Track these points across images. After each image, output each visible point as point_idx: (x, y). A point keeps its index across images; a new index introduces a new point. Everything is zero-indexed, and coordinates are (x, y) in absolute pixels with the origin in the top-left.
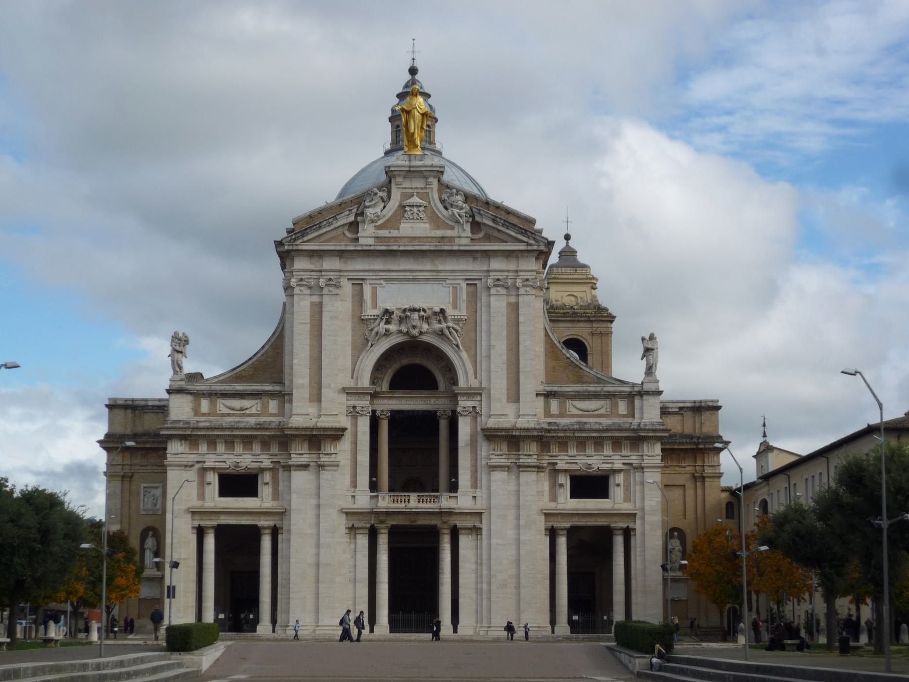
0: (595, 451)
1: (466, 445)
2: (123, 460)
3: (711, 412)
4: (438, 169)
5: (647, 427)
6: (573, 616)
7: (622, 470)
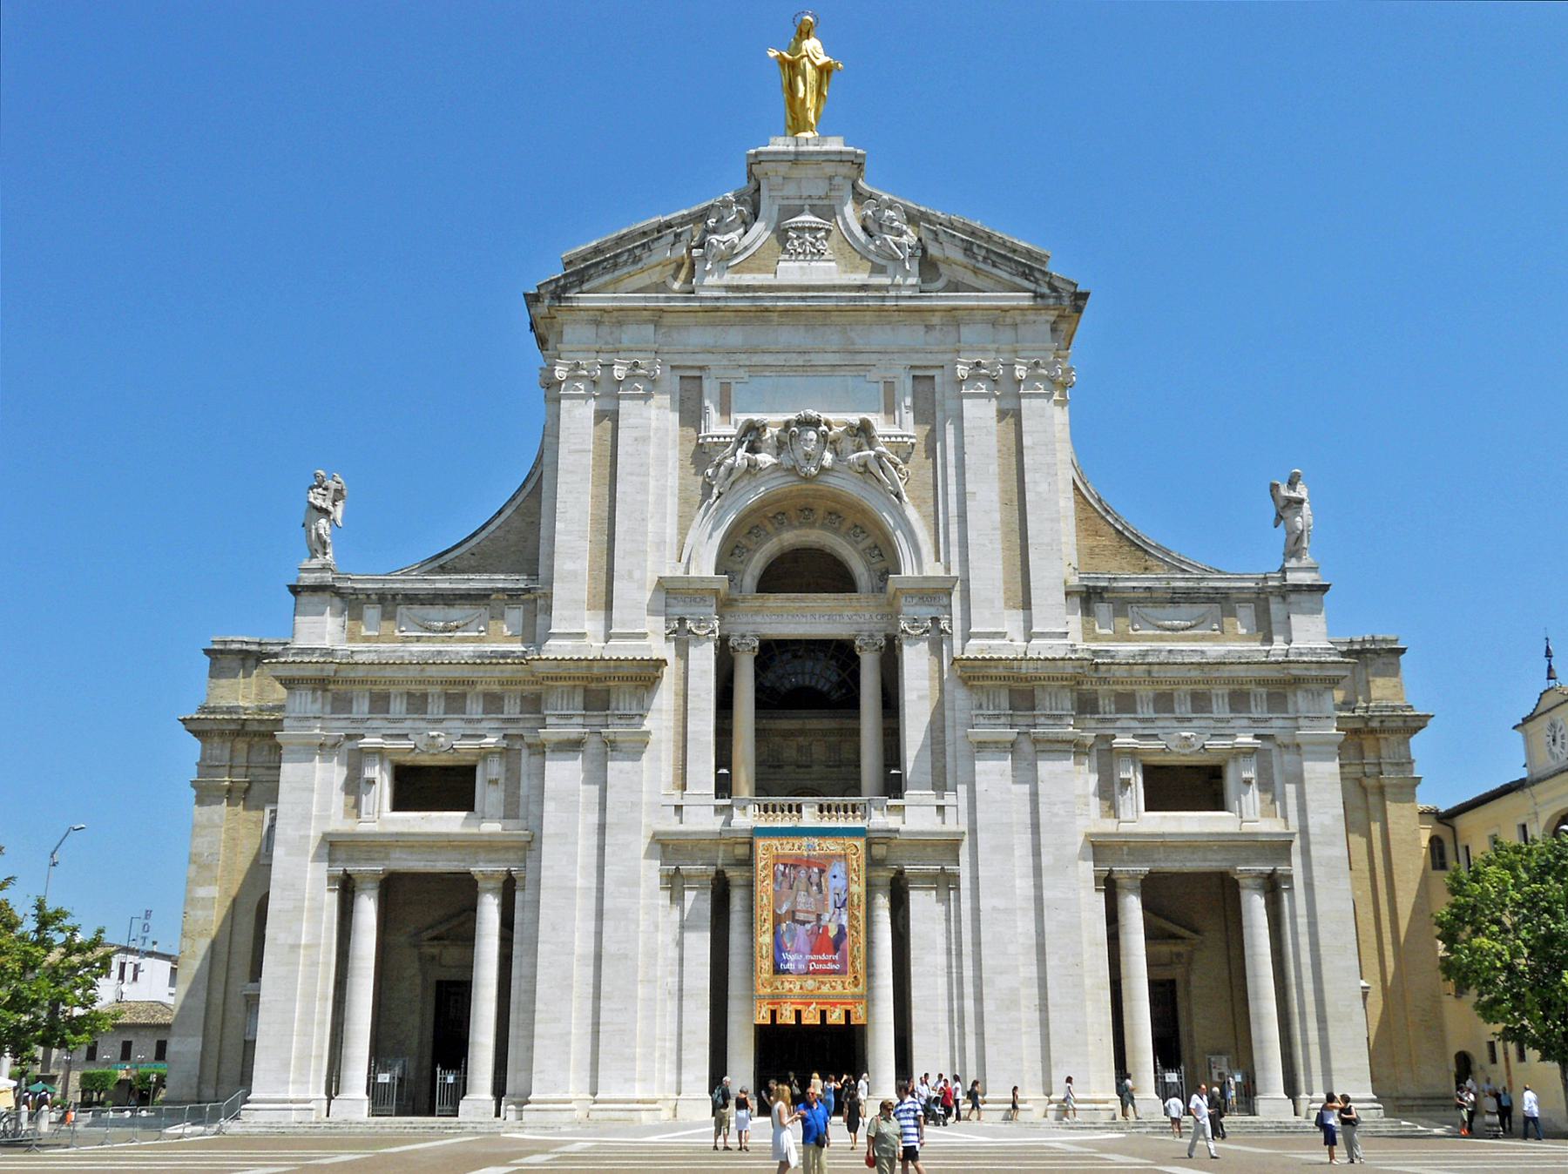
0: (1194, 712)
1: (920, 698)
2: (231, 759)
3: (1385, 660)
4: (852, 158)
5: (1306, 659)
6: (1167, 1075)
7: (1250, 752)
